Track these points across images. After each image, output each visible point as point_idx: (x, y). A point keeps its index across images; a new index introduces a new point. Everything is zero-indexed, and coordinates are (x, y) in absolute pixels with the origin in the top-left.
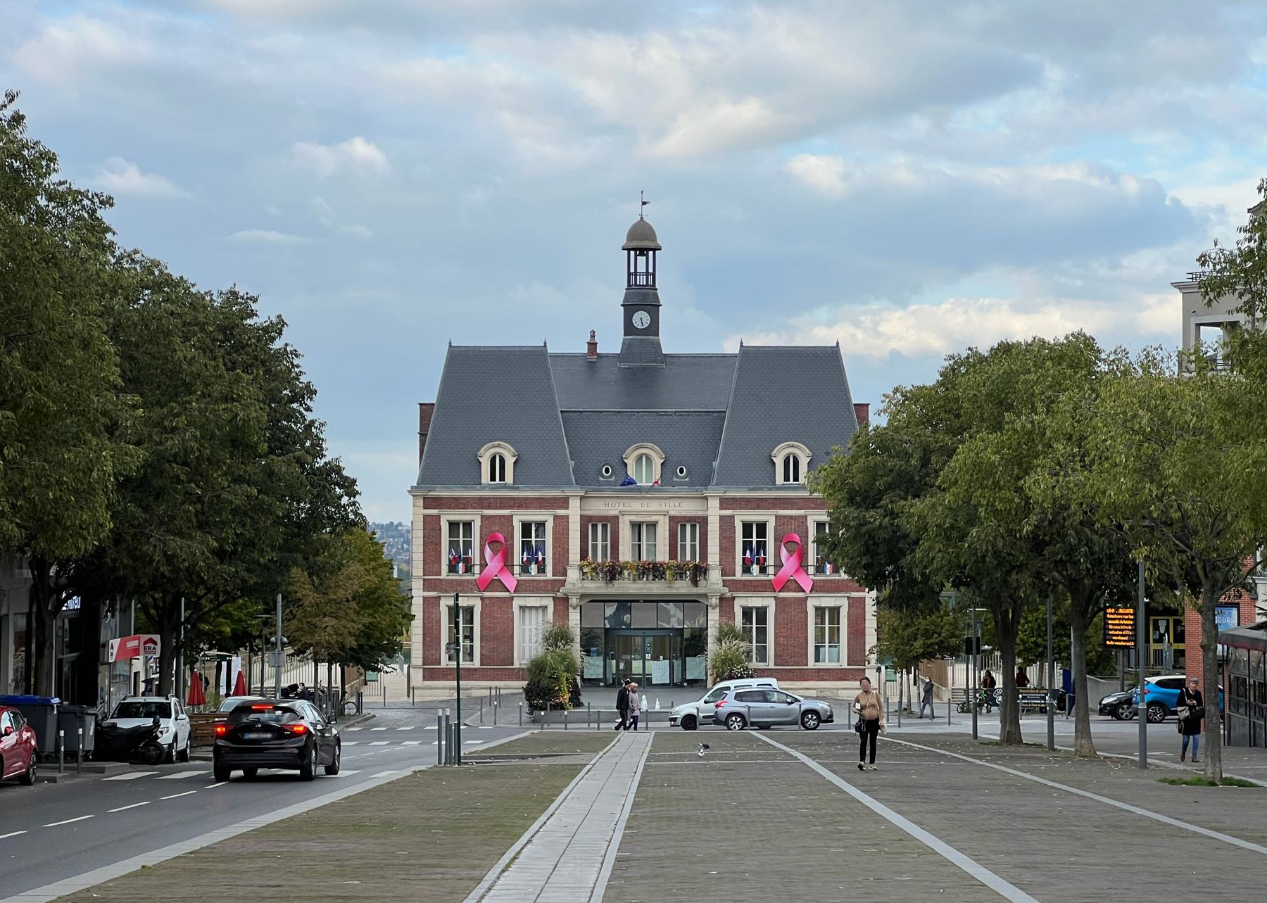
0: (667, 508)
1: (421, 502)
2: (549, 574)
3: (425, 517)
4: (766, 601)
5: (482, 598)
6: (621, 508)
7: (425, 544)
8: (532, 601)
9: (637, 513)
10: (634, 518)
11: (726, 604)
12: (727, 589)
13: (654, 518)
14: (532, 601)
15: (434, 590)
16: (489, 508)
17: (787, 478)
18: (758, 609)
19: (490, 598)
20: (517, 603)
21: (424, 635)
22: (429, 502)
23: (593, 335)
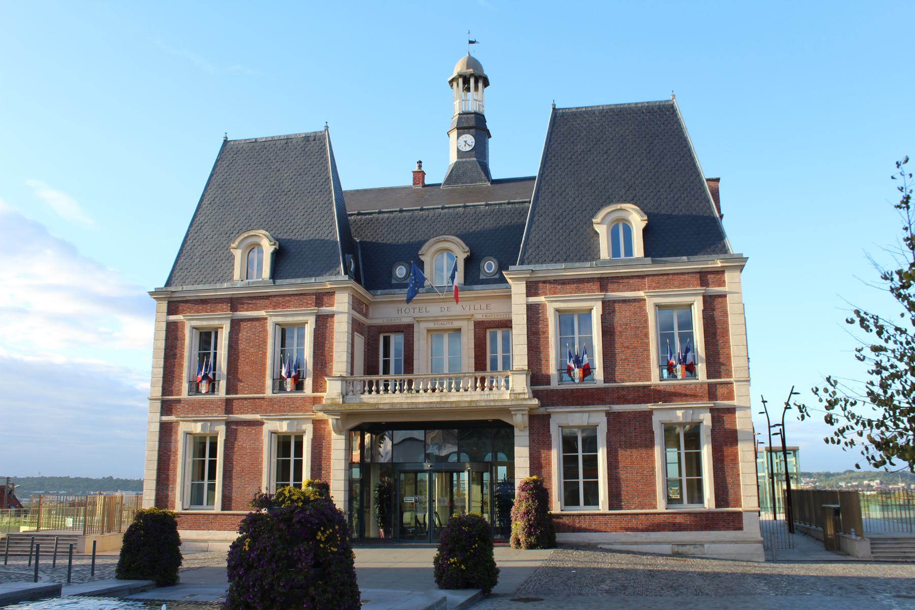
0: (472, 312)
1: (164, 306)
4: (596, 417)
6: (417, 314)
9: (435, 320)
10: (431, 325)
11: (539, 425)
12: (536, 402)
13: (456, 324)
17: (615, 251)
18: (583, 429)
22: (173, 307)
23: (420, 162)
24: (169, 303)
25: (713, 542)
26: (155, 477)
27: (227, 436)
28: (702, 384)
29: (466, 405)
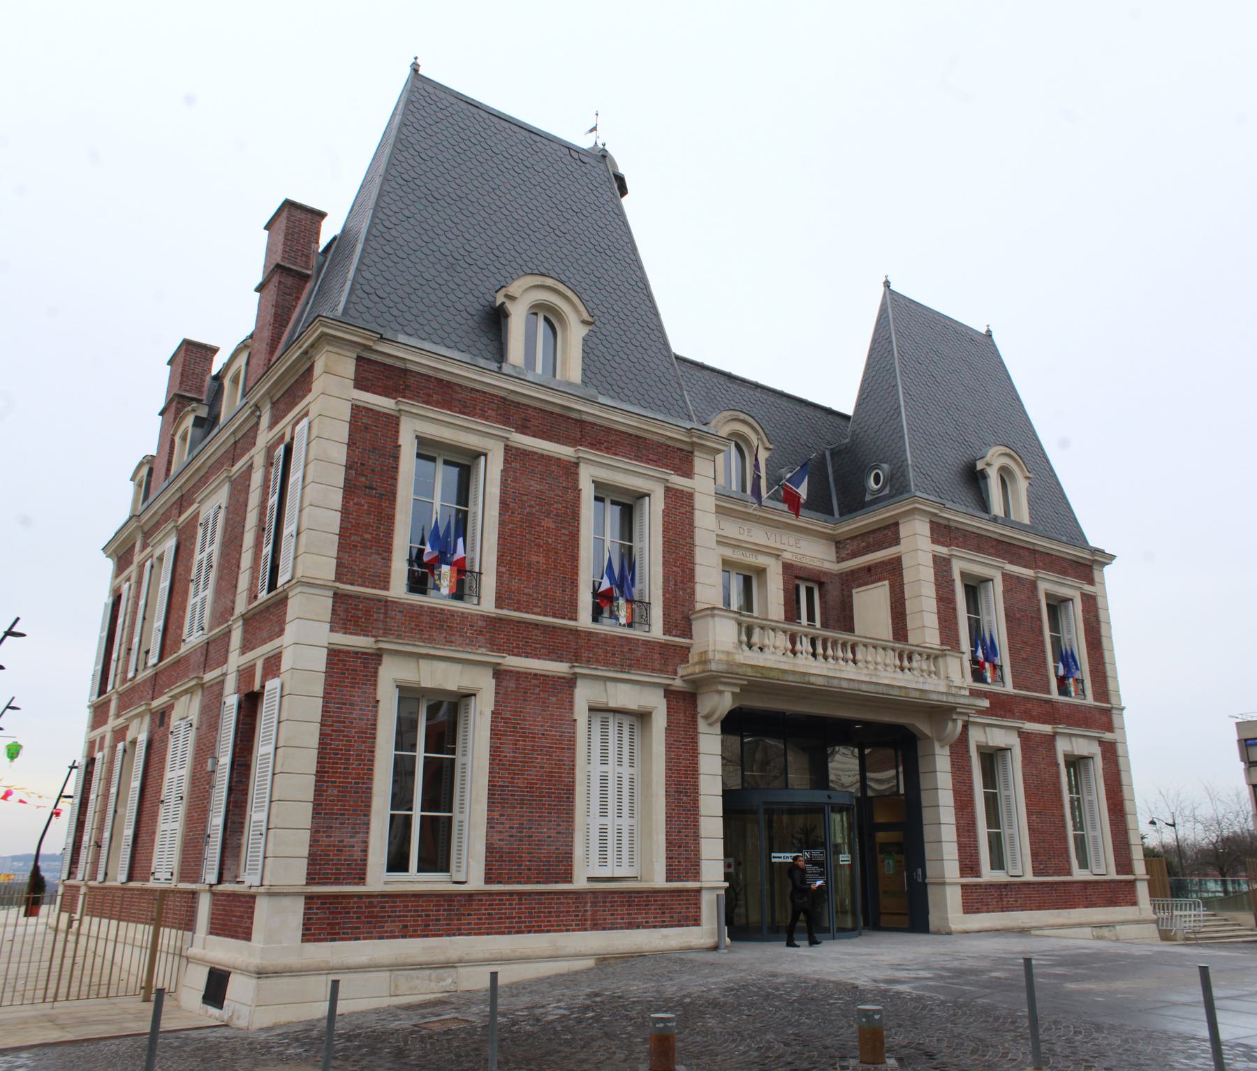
2: (656, 631)
3: (358, 411)
5: (500, 674)
7: (350, 489)
8: (625, 696)
10: (729, 553)
14: (625, 696)
15: (364, 632)
16: (523, 429)
19: (519, 675)
20: (584, 695)
21: (320, 774)
24: (359, 359)
25: (1123, 923)
26: (310, 795)
27: (497, 703)
28: (1090, 708)
29: (917, 694)
